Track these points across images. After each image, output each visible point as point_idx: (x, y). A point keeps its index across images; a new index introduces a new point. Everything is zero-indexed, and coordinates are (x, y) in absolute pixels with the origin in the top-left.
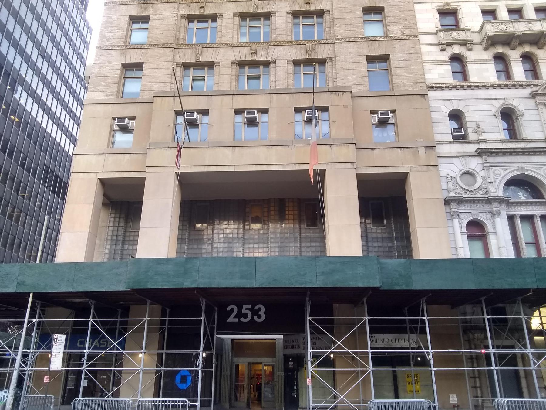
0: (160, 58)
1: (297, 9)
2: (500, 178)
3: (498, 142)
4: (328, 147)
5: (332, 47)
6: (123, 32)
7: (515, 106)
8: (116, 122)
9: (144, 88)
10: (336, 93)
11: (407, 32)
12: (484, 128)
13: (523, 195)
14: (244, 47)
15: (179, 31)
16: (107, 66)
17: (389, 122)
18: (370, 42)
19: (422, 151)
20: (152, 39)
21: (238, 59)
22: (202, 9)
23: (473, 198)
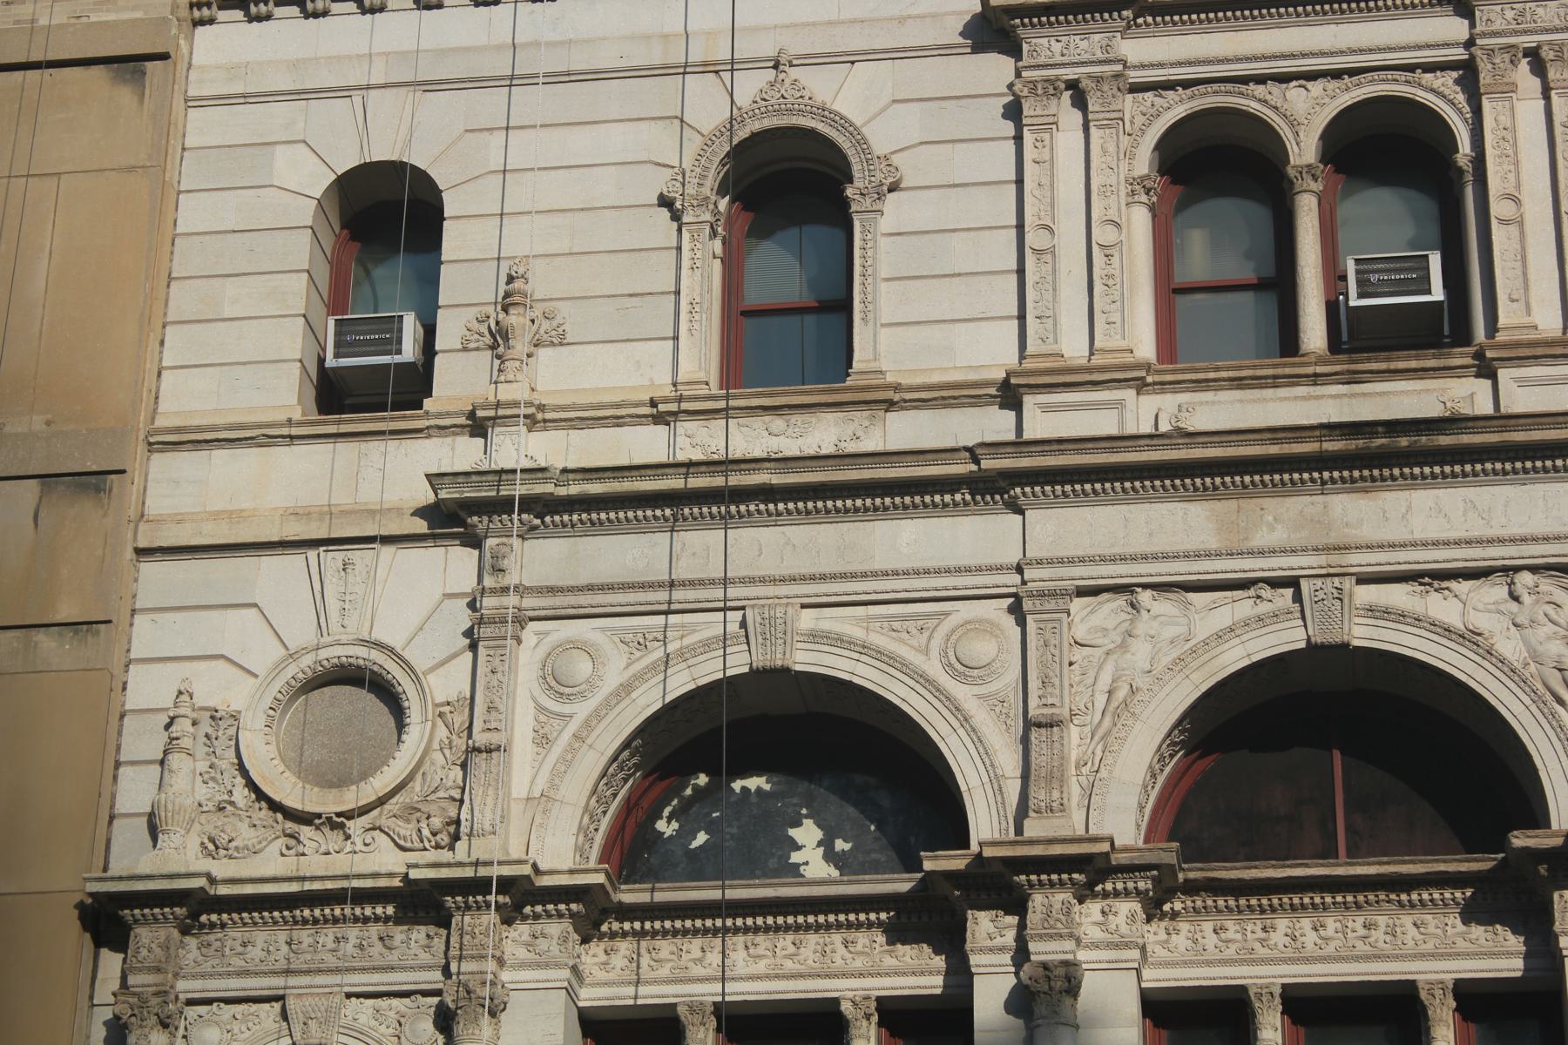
2: (582, 710)
3: (638, 419)
7: (843, 123)
12: (564, 309)
13: (826, 844)
23: (303, 879)
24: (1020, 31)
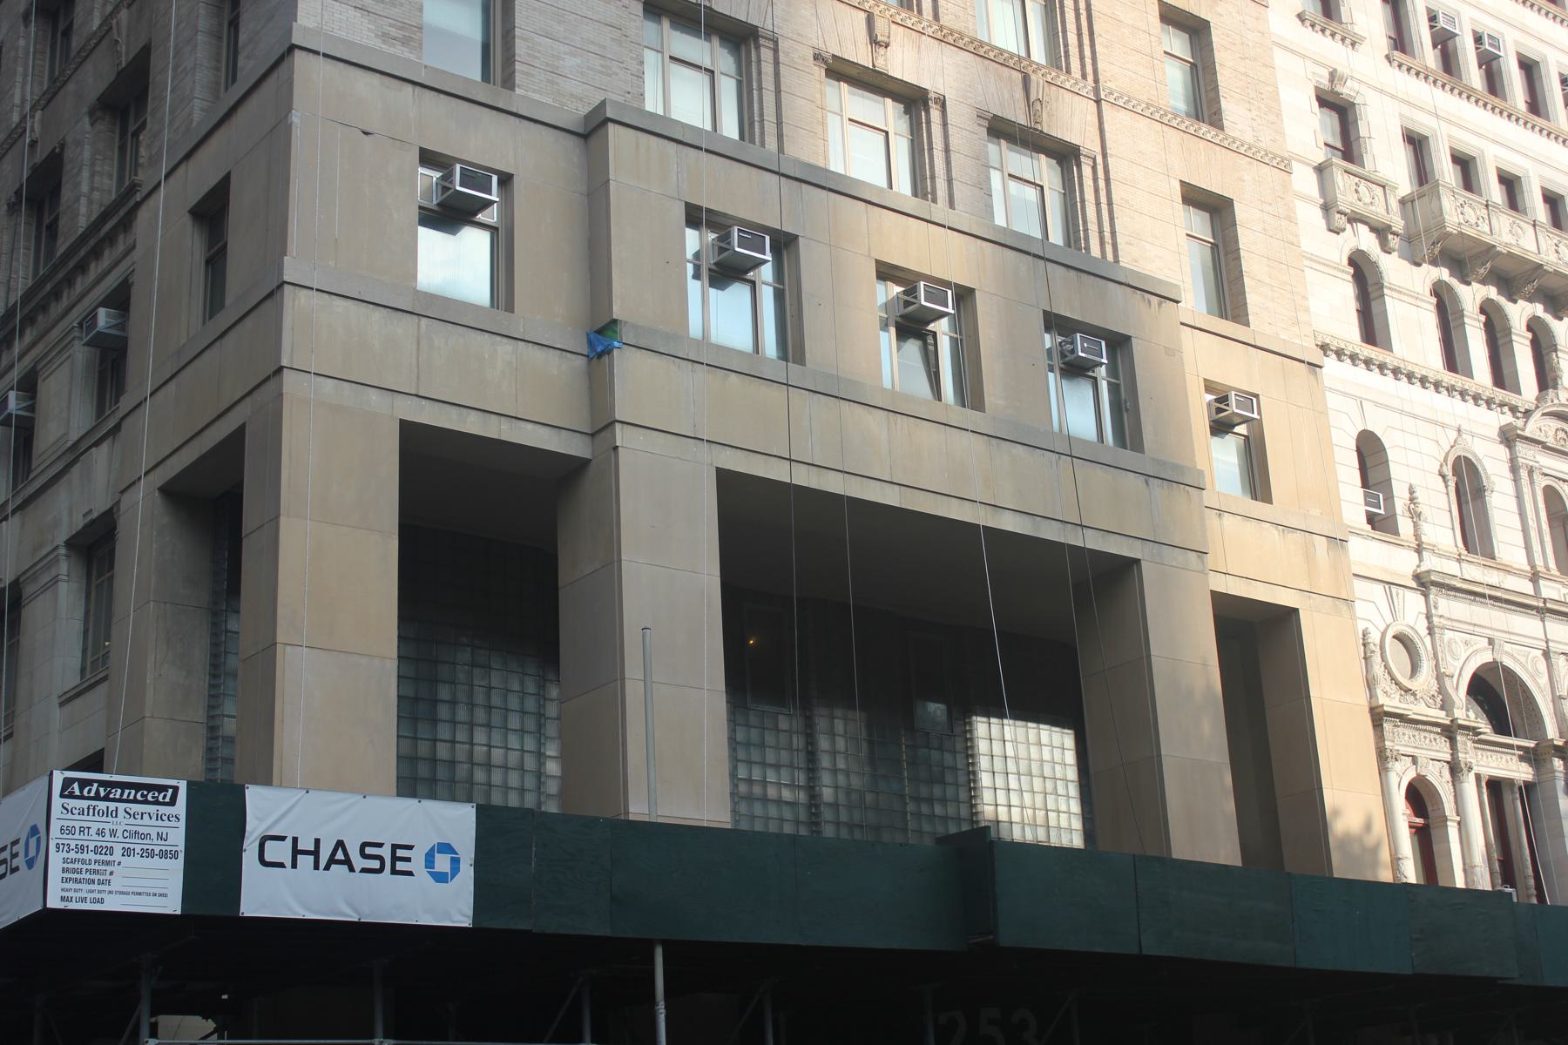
9: (529, 55)
19: (1321, 543)
24: (1517, 443)
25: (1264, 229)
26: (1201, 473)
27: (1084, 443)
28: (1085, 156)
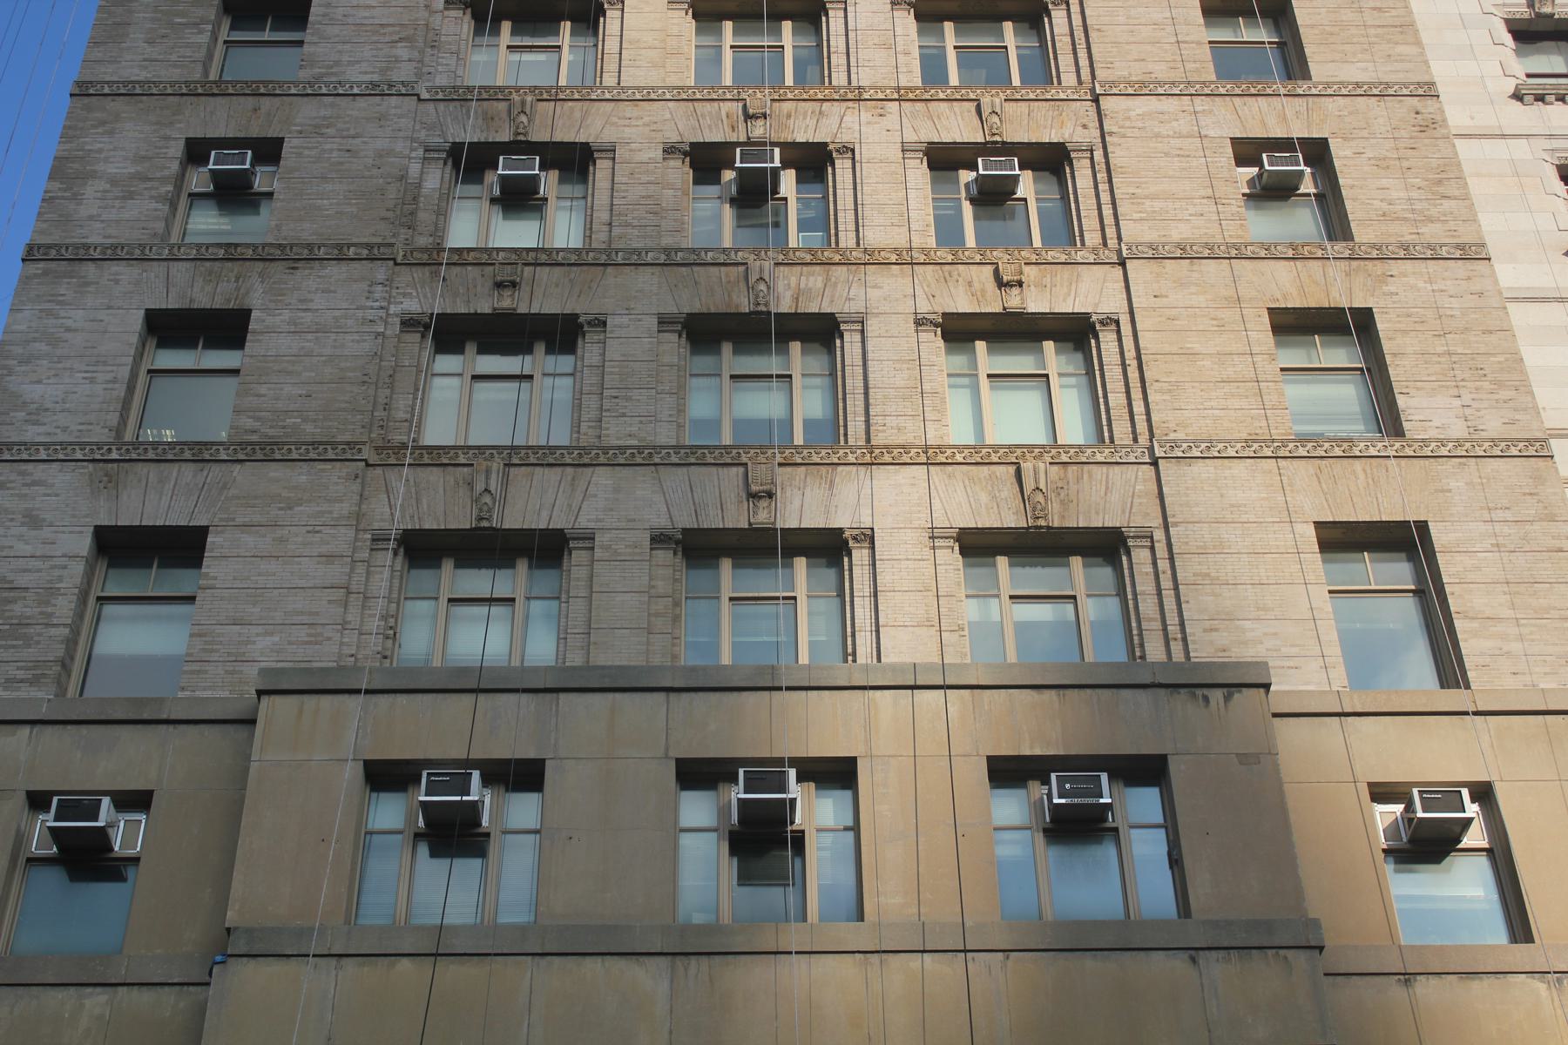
0: (290, 508)
1: (963, 304)
4: (1177, 965)
5: (1145, 481)
6: (115, 380)
8: (49, 819)
9: (204, 650)
10: (1194, 695)
11: (1493, 425)
14: (714, 469)
15: (391, 387)
16: (20, 537)
17: (1466, 842)
18: (1324, 462)
20: (258, 419)
21: (686, 521)
22: (507, 293)
25: (1498, 545)
26: (1316, 924)
27: (1159, 924)
28: (1133, 537)
